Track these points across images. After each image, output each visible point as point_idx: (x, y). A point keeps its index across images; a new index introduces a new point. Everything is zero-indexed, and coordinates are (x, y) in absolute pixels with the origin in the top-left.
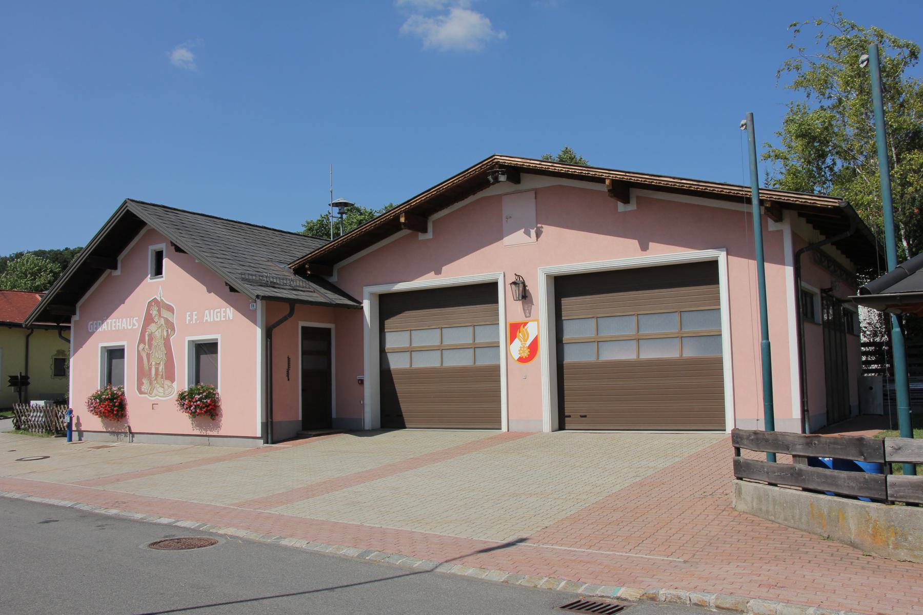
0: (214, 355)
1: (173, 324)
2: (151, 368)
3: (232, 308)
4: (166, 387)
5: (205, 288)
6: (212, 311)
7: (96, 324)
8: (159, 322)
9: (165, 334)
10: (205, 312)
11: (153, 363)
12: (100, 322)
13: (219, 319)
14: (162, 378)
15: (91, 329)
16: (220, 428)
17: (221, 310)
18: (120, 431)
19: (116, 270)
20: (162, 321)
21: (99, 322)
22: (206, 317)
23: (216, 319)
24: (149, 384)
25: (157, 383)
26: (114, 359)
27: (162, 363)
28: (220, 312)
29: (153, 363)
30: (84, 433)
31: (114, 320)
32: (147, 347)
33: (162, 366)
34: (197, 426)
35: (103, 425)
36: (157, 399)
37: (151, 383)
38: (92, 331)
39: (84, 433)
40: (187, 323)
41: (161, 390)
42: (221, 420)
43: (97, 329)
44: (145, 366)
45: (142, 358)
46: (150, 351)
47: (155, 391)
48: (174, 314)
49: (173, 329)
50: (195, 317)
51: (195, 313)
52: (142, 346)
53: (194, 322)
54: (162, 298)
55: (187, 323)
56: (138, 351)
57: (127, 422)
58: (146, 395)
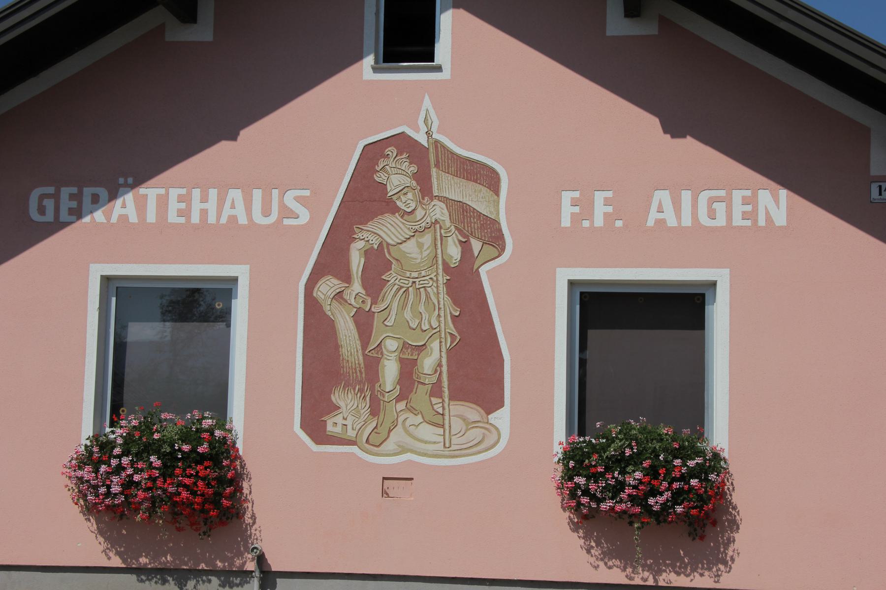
0: (691, 334)
1: (495, 223)
2: (378, 361)
3: (783, 193)
4: (457, 425)
5: (653, 122)
6: (686, 196)
7: (77, 197)
8: (420, 213)
9: (454, 252)
10: (650, 197)
11: (392, 345)
12: (103, 192)
13: (721, 221)
14: (436, 391)
15: (42, 210)
16: (725, 563)
17: (58, 191)
18: (202, 566)
19: (195, 25)
20: (439, 211)
21: (88, 191)
22: (233, 207)
23: (704, 220)
24: (365, 411)
25: (411, 409)
26: (591, 328)
27: (435, 345)
28: (56, 197)
29: (392, 345)
30: (280, 582)
31: (174, 193)
32: (357, 287)
33: (436, 355)
34: (607, 555)
35: (104, 545)
36: (410, 462)
37: (375, 411)
38: (49, 217)
39: (280, 582)
40: (566, 222)
41: (427, 432)
42: (730, 541)
43: (78, 213)
44: (344, 351)
45: (331, 325)
46: (374, 302)
47: (397, 435)
48: (497, 192)
49: (496, 240)
50: (600, 210)
51: (599, 197)
52: (327, 287)
53: (599, 221)
54: (436, 136)
55: (566, 222)
56: (312, 306)
57: (244, 535)
58: (354, 449)
